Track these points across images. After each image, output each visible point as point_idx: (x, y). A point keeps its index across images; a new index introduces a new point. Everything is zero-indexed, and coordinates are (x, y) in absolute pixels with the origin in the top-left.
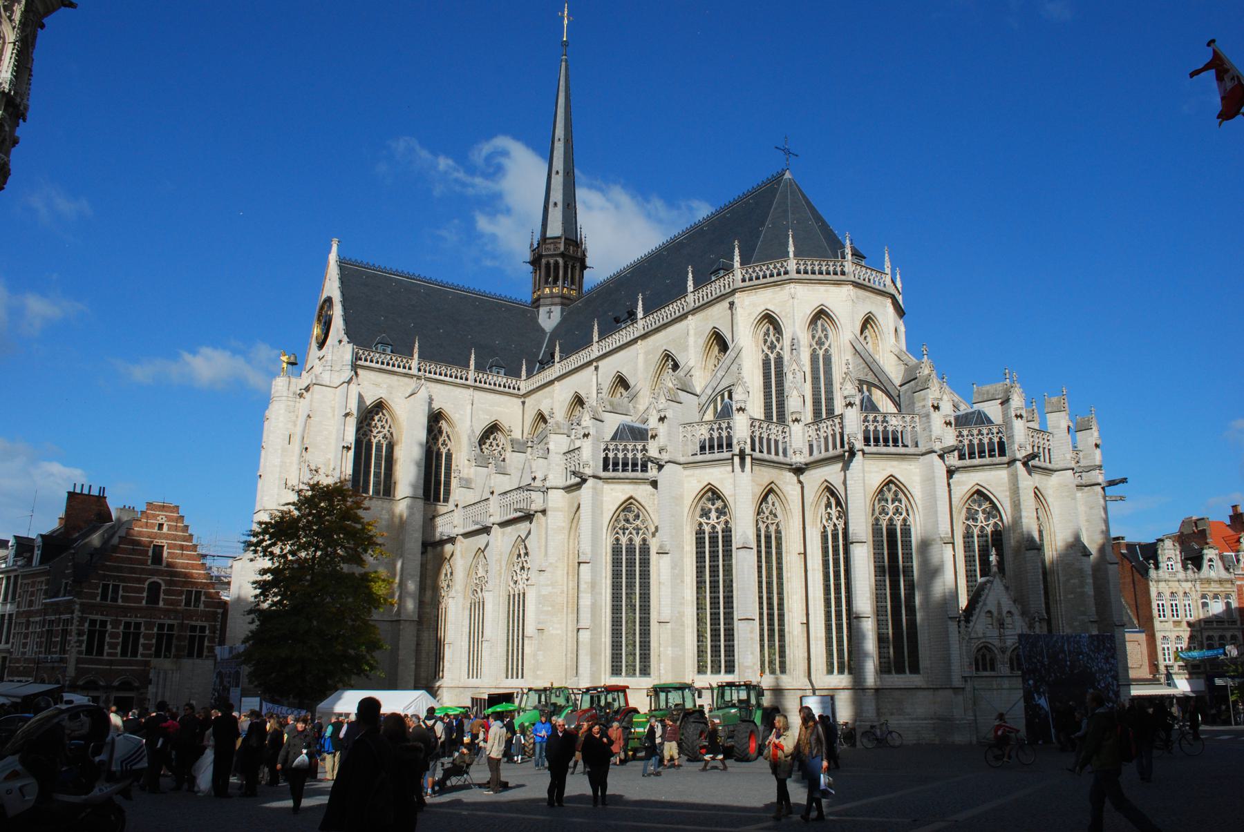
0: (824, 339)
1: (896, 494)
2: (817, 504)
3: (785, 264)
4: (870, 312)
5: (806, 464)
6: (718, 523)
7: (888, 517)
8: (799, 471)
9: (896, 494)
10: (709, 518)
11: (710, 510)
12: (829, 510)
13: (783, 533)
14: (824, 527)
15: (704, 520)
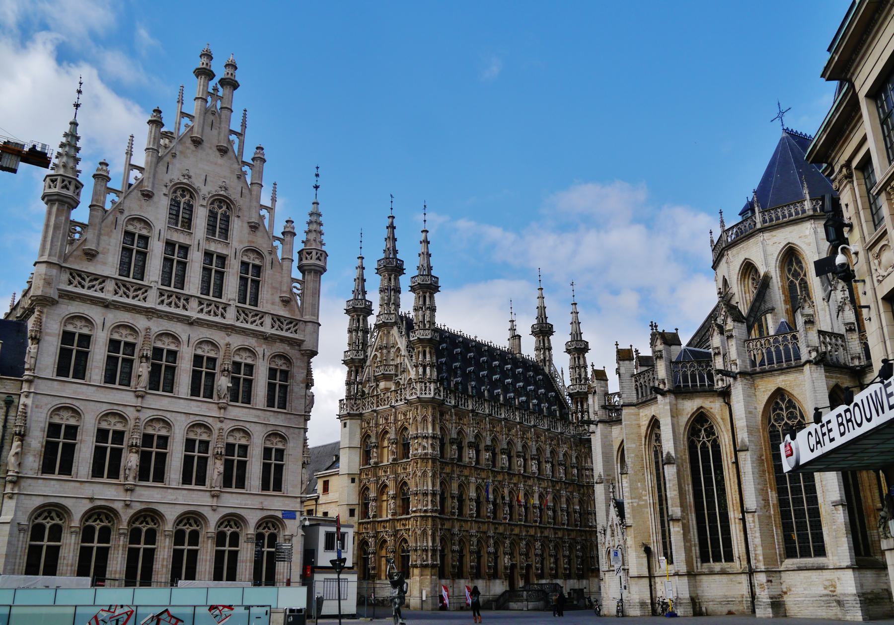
0: (799, 270)
9: (790, 401)
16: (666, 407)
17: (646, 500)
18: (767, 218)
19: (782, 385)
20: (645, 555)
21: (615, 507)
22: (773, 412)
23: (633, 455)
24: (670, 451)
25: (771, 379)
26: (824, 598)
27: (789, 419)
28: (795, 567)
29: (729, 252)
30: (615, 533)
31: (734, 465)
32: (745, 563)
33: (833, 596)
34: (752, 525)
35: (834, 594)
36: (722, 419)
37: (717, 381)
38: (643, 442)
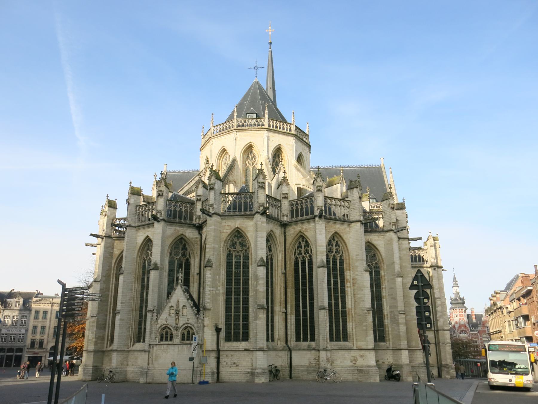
0: (278, 162)
1: (337, 242)
2: (294, 246)
3: (262, 120)
4: (301, 153)
5: (289, 222)
6: (241, 251)
7: (333, 254)
8: (284, 225)
9: (337, 242)
10: (235, 248)
11: (236, 243)
12: (300, 249)
13: (274, 260)
14: (297, 258)
15: (232, 249)
16: (263, 225)
17: (219, 290)
18: (271, 124)
19: (338, 231)
20: (215, 333)
21: (184, 292)
22: (328, 246)
23: (216, 253)
24: (263, 257)
25: (333, 225)
26: (351, 368)
27: (336, 252)
28: (336, 347)
29: (238, 133)
30: (180, 313)
31: (284, 275)
32: (283, 343)
33: (356, 367)
34: (326, 318)
35: (356, 365)
36: (280, 242)
37: (283, 216)
38: (222, 245)
